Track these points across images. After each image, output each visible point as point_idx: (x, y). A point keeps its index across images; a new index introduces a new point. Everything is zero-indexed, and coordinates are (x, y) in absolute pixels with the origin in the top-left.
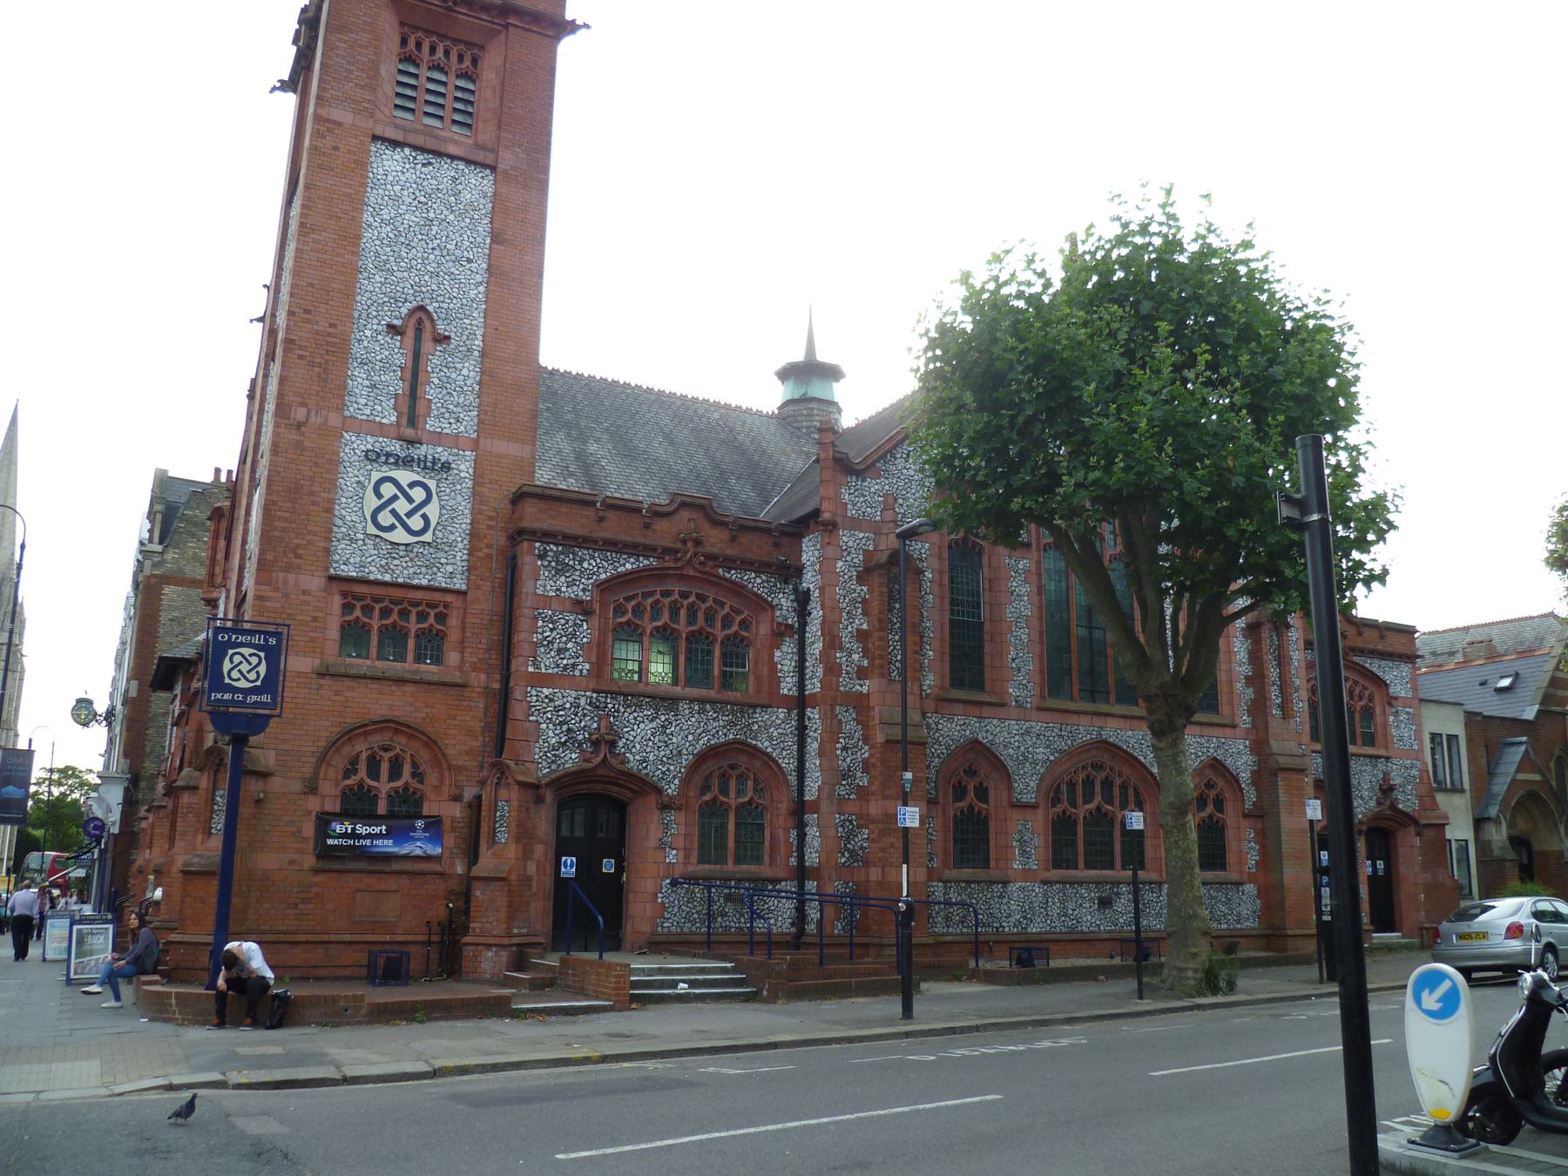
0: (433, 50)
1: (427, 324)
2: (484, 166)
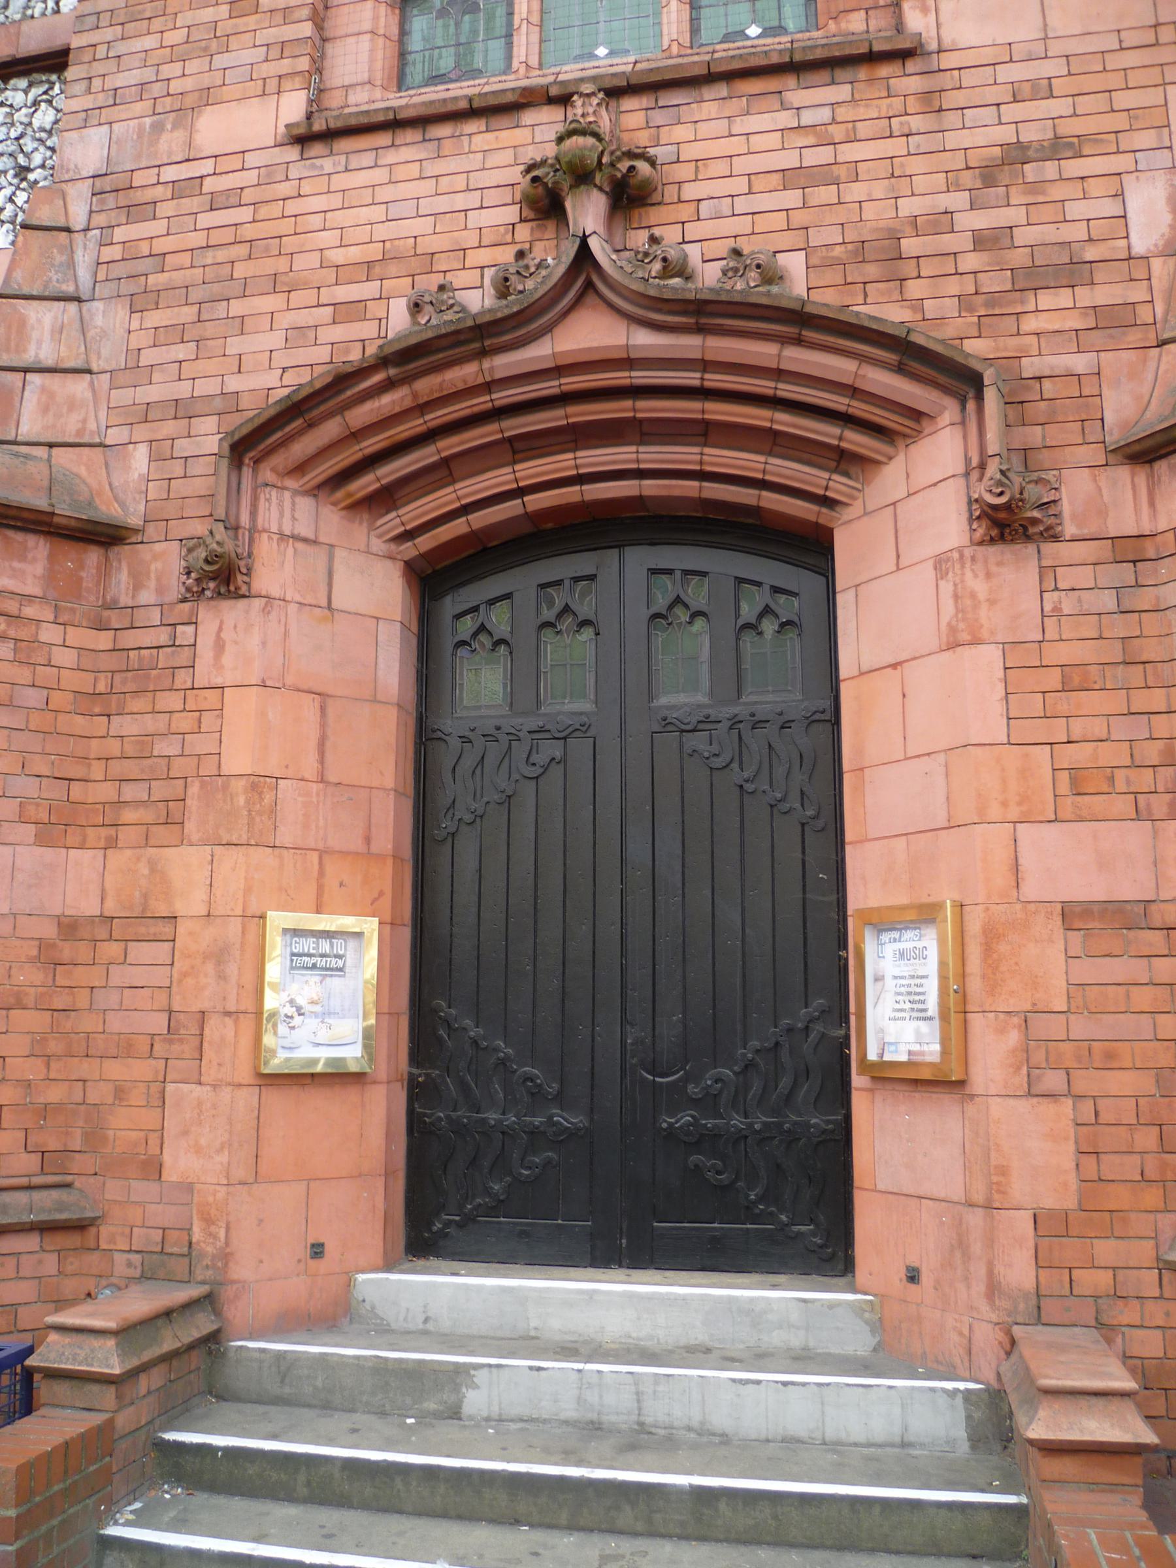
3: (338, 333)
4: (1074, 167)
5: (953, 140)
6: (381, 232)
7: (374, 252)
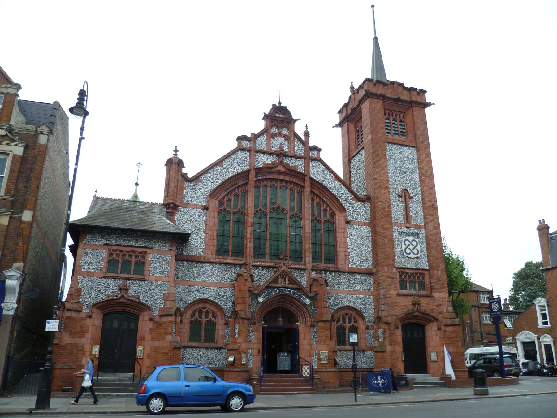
0: (392, 115)
1: (407, 194)
2: (412, 147)
3: (402, 311)
4: (441, 306)
5: (436, 303)
6: (404, 303)
7: (403, 305)
